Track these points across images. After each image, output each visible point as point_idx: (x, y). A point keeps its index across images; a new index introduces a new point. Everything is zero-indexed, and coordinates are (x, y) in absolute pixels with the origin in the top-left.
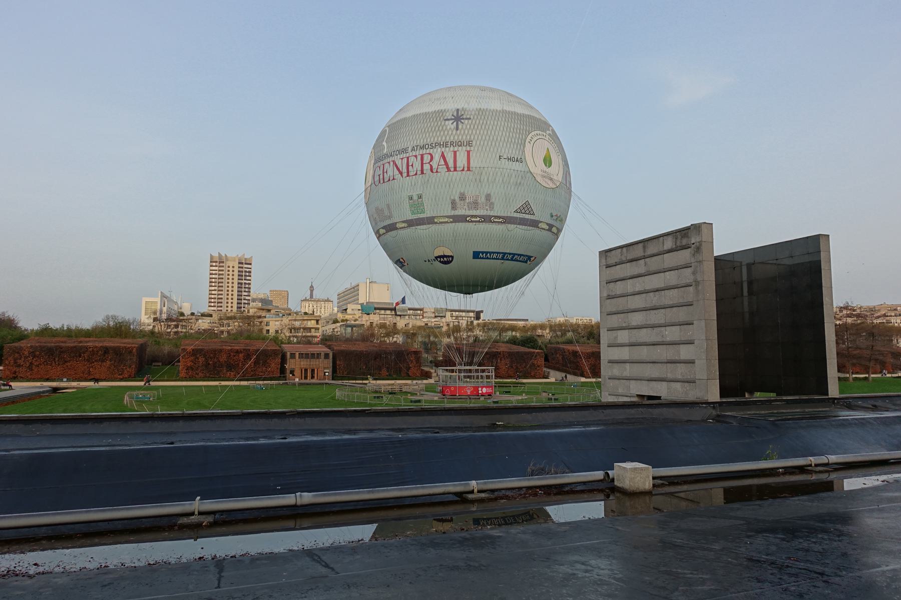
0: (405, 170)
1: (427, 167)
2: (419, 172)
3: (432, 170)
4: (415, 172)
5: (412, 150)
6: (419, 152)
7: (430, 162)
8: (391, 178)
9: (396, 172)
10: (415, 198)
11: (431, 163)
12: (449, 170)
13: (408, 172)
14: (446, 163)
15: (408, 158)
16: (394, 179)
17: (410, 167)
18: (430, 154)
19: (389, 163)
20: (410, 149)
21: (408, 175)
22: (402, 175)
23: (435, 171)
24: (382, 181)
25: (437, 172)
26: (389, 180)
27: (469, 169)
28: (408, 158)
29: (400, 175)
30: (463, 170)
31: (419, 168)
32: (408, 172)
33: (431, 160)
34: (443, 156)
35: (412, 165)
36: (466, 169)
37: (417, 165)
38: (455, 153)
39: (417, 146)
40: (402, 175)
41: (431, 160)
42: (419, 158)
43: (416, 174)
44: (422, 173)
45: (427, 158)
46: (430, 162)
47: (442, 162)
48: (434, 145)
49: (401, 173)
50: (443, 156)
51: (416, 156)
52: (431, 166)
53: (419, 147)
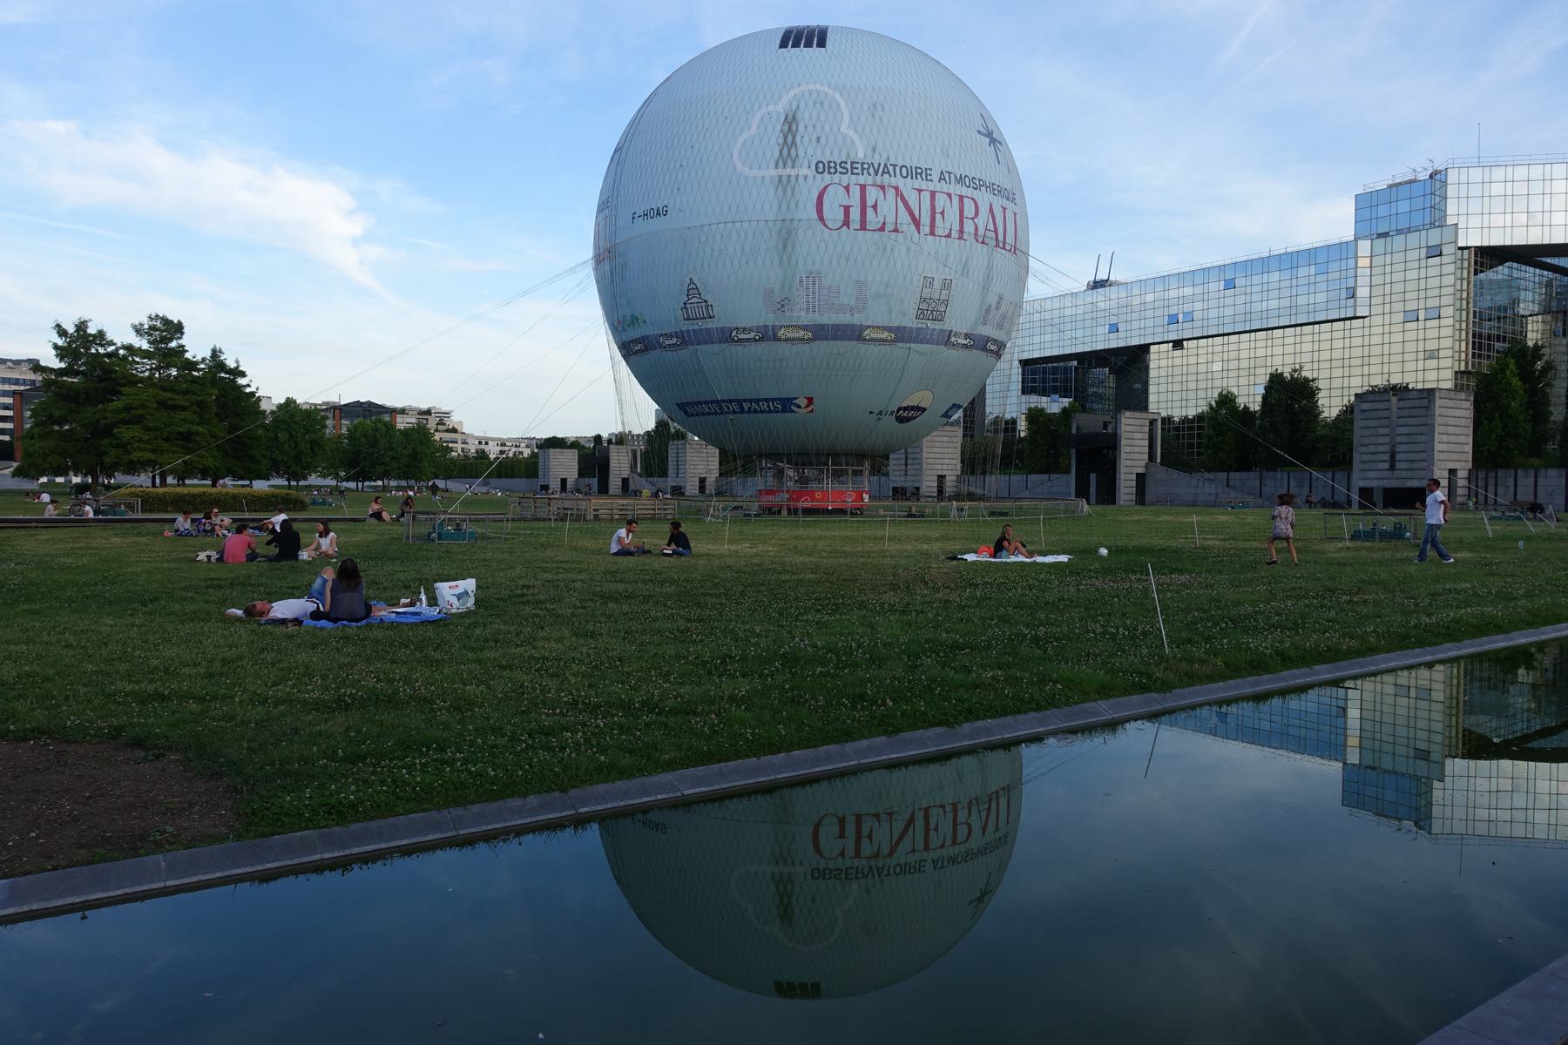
0: (925, 220)
1: (969, 227)
2: (955, 234)
4: (947, 232)
5: (940, 179)
6: (957, 189)
8: (889, 227)
10: (937, 284)
11: (976, 220)
13: (933, 226)
14: (996, 231)
15: (933, 194)
21: (932, 233)
26: (882, 229)
28: (933, 194)
29: (913, 227)
31: (956, 226)
32: (933, 226)
34: (991, 210)
35: (942, 213)
38: (1004, 209)
39: (950, 173)
42: (956, 200)
43: (949, 236)
49: (917, 223)
50: (991, 210)
51: (949, 195)
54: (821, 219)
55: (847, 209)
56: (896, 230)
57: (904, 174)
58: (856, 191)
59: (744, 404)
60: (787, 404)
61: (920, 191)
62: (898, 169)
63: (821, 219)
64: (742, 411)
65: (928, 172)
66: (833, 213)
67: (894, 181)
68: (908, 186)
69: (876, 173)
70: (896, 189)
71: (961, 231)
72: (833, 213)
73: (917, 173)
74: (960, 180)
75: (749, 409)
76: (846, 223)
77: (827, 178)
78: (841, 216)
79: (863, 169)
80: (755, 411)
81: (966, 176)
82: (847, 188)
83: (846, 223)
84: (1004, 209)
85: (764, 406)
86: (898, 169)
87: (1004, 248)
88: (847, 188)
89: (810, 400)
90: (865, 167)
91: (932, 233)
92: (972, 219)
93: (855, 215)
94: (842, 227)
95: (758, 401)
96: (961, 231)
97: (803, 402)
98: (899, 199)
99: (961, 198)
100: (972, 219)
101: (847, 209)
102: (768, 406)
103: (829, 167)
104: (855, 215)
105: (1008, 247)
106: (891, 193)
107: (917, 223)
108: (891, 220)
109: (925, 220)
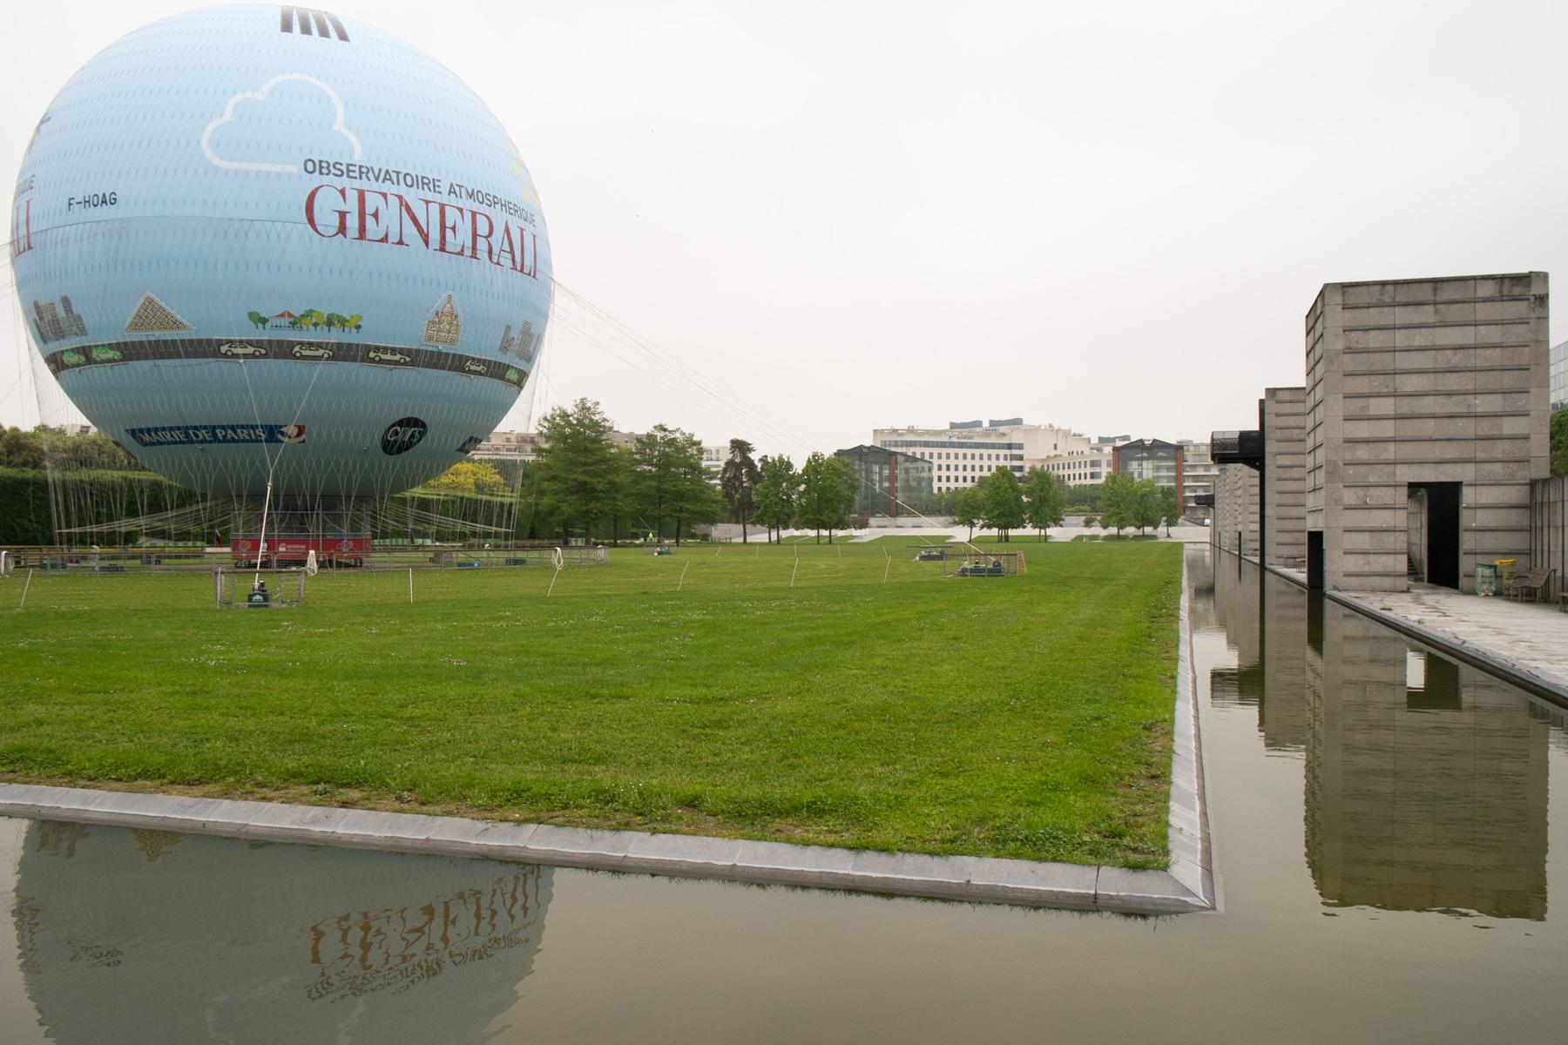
0: (435, 235)
1: (482, 244)
2: (468, 252)
4: (459, 249)
5: (450, 192)
8: (394, 238)
14: (512, 252)
16: (401, 242)
17: (449, 233)
22: (427, 243)
25: (499, 264)
26: (385, 239)
28: (442, 208)
31: (469, 243)
35: (454, 229)
37: (465, 235)
39: (460, 186)
40: (427, 243)
42: (468, 216)
43: (461, 253)
44: (474, 256)
47: (506, 247)
51: (461, 210)
54: (311, 221)
55: (343, 215)
56: (401, 242)
57: (409, 183)
58: (353, 197)
59: (218, 431)
60: (273, 433)
61: (427, 202)
62: (401, 176)
63: (311, 221)
64: (215, 439)
65: (437, 183)
66: (327, 218)
67: (402, 190)
68: (413, 197)
69: (377, 179)
70: (400, 197)
71: (474, 248)
72: (327, 218)
73: (423, 183)
74: (471, 195)
75: (224, 437)
76: (342, 229)
77: (316, 179)
78: (335, 220)
79: (361, 173)
80: (233, 440)
81: (478, 192)
82: (343, 192)
83: (342, 229)
84: (522, 230)
85: (242, 434)
86: (401, 176)
87: (522, 271)
88: (343, 192)
89: (301, 430)
90: (364, 172)
91: (442, 249)
92: (486, 237)
93: (352, 222)
94: (337, 234)
95: (233, 428)
96: (474, 248)
97: (292, 430)
98: (403, 209)
99: (474, 214)
100: (486, 237)
101: (343, 215)
102: (249, 435)
103: (321, 167)
104: (352, 222)
105: (526, 270)
106: (394, 203)
109: (435, 235)
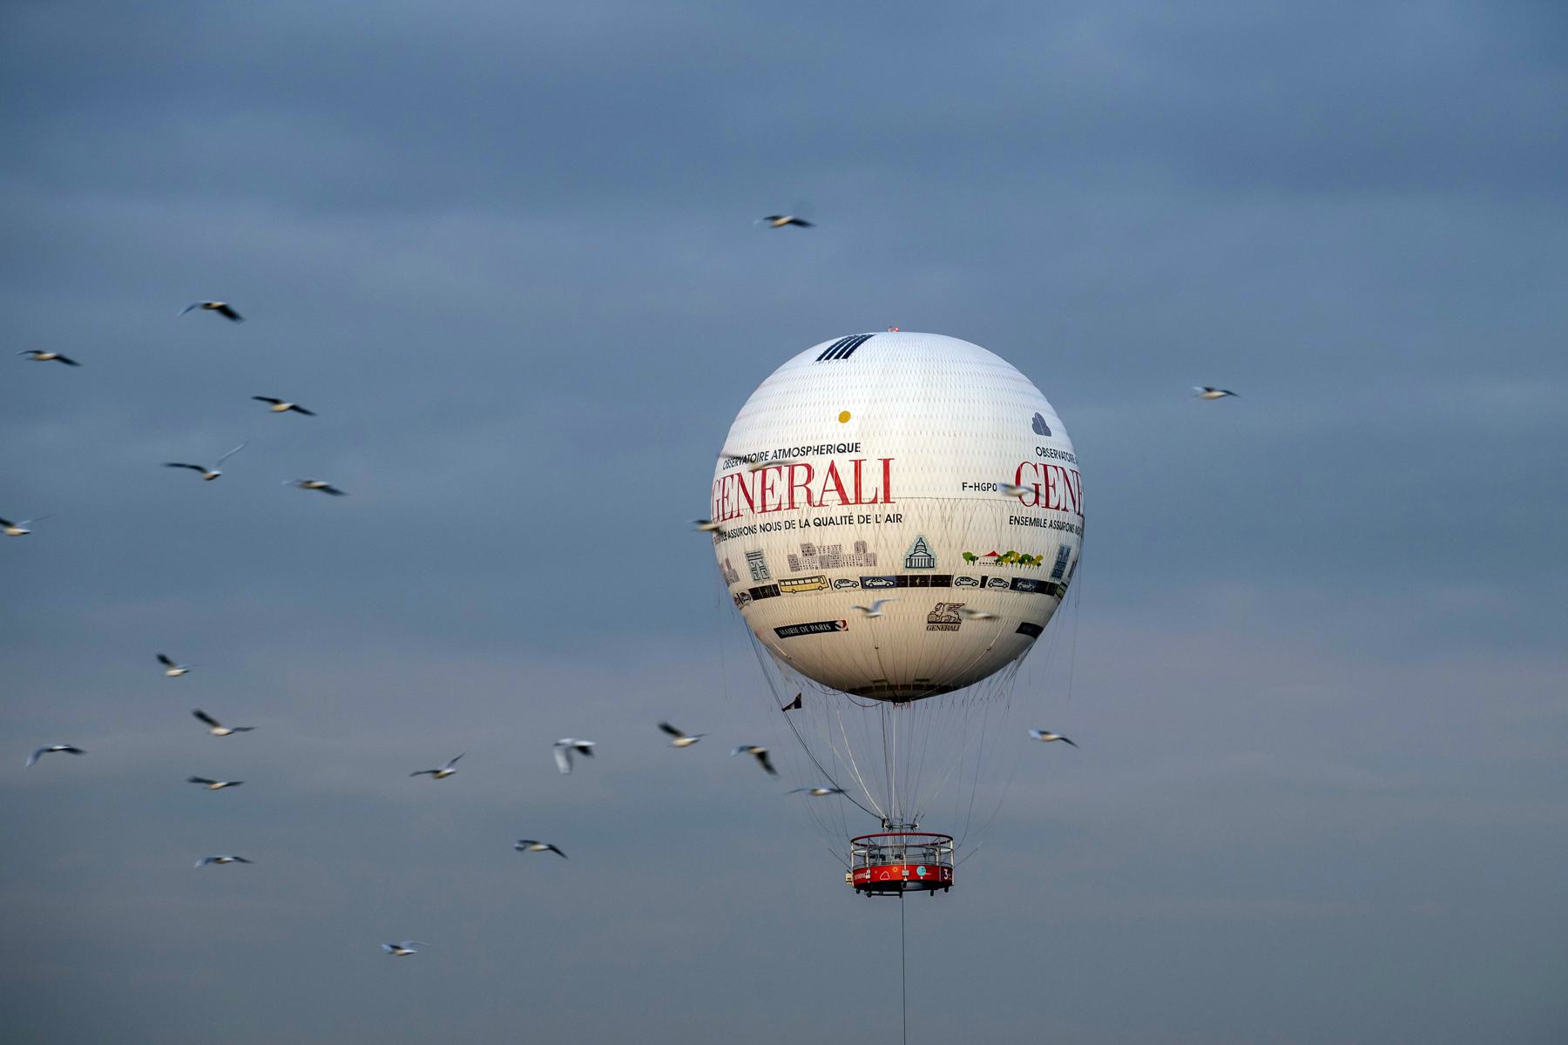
0: (758, 503)
1: (800, 494)
2: (785, 500)
3: (809, 501)
7: (807, 483)
8: (735, 514)
9: (744, 504)
12: (845, 501)
13: (764, 505)
14: (839, 487)
16: (738, 515)
17: (768, 493)
18: (809, 467)
19: (732, 476)
20: (771, 455)
22: (752, 508)
23: (816, 498)
24: (721, 518)
25: (821, 505)
27: (887, 499)
30: (875, 501)
32: (764, 505)
33: (809, 479)
34: (832, 469)
35: (772, 489)
36: (881, 495)
37: (782, 487)
40: (752, 508)
41: (809, 479)
43: (779, 509)
44: (792, 505)
45: (800, 475)
46: (807, 483)
47: (831, 484)
48: (805, 450)
49: (751, 503)
50: (832, 469)
52: (809, 490)
53: (782, 452)
92: (804, 485)
100: (804, 485)
105: (867, 495)
107: (751, 503)
108: (735, 509)
109: (758, 503)
